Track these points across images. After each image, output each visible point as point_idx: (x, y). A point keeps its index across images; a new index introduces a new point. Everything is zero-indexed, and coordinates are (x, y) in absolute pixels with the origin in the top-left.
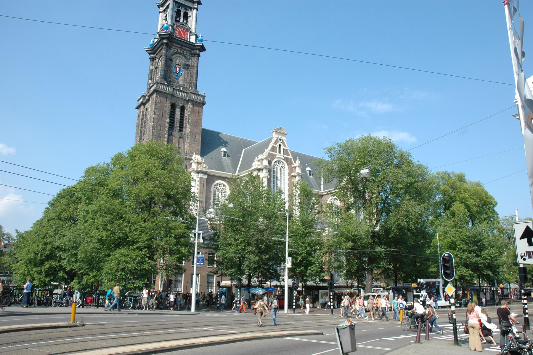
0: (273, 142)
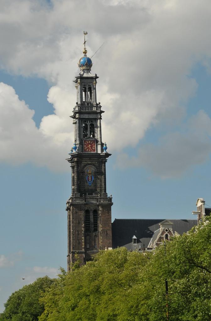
0: (160, 233)
